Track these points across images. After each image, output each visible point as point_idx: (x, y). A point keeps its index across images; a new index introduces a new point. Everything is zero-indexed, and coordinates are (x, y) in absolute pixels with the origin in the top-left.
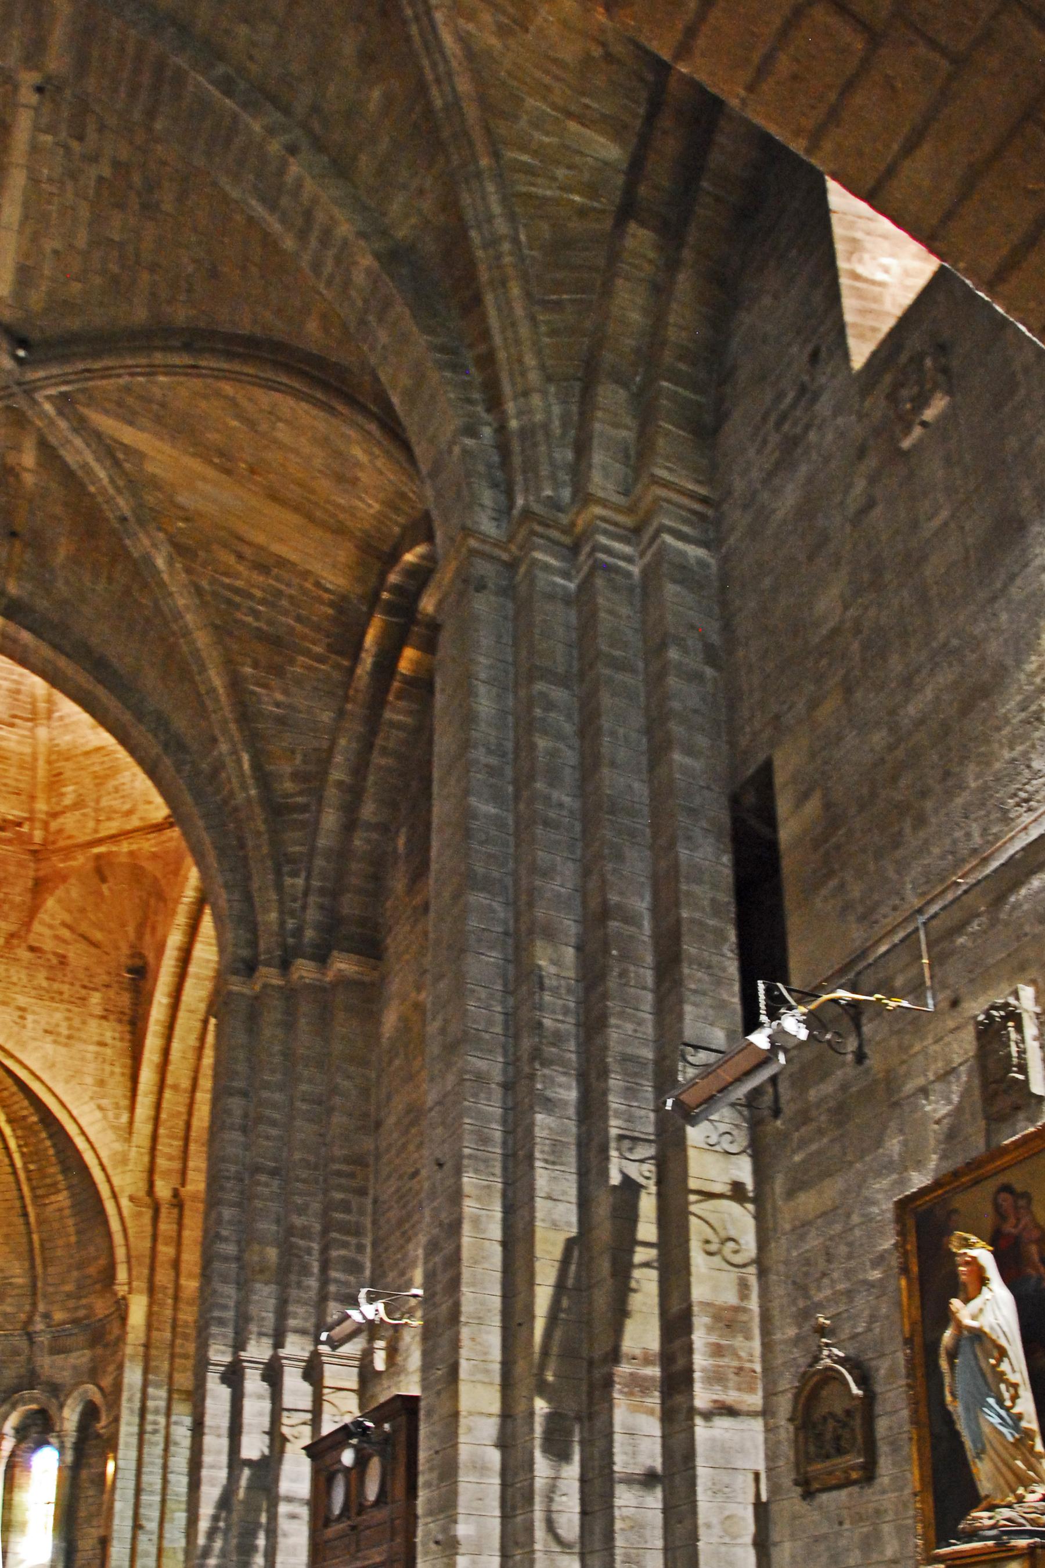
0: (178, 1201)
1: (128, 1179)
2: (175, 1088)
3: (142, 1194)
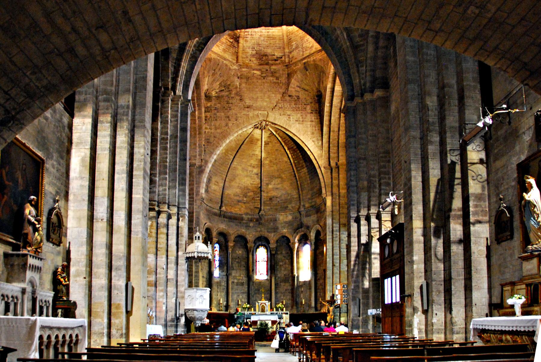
0: (338, 167)
1: (323, 162)
2: (333, 131)
3: (327, 165)
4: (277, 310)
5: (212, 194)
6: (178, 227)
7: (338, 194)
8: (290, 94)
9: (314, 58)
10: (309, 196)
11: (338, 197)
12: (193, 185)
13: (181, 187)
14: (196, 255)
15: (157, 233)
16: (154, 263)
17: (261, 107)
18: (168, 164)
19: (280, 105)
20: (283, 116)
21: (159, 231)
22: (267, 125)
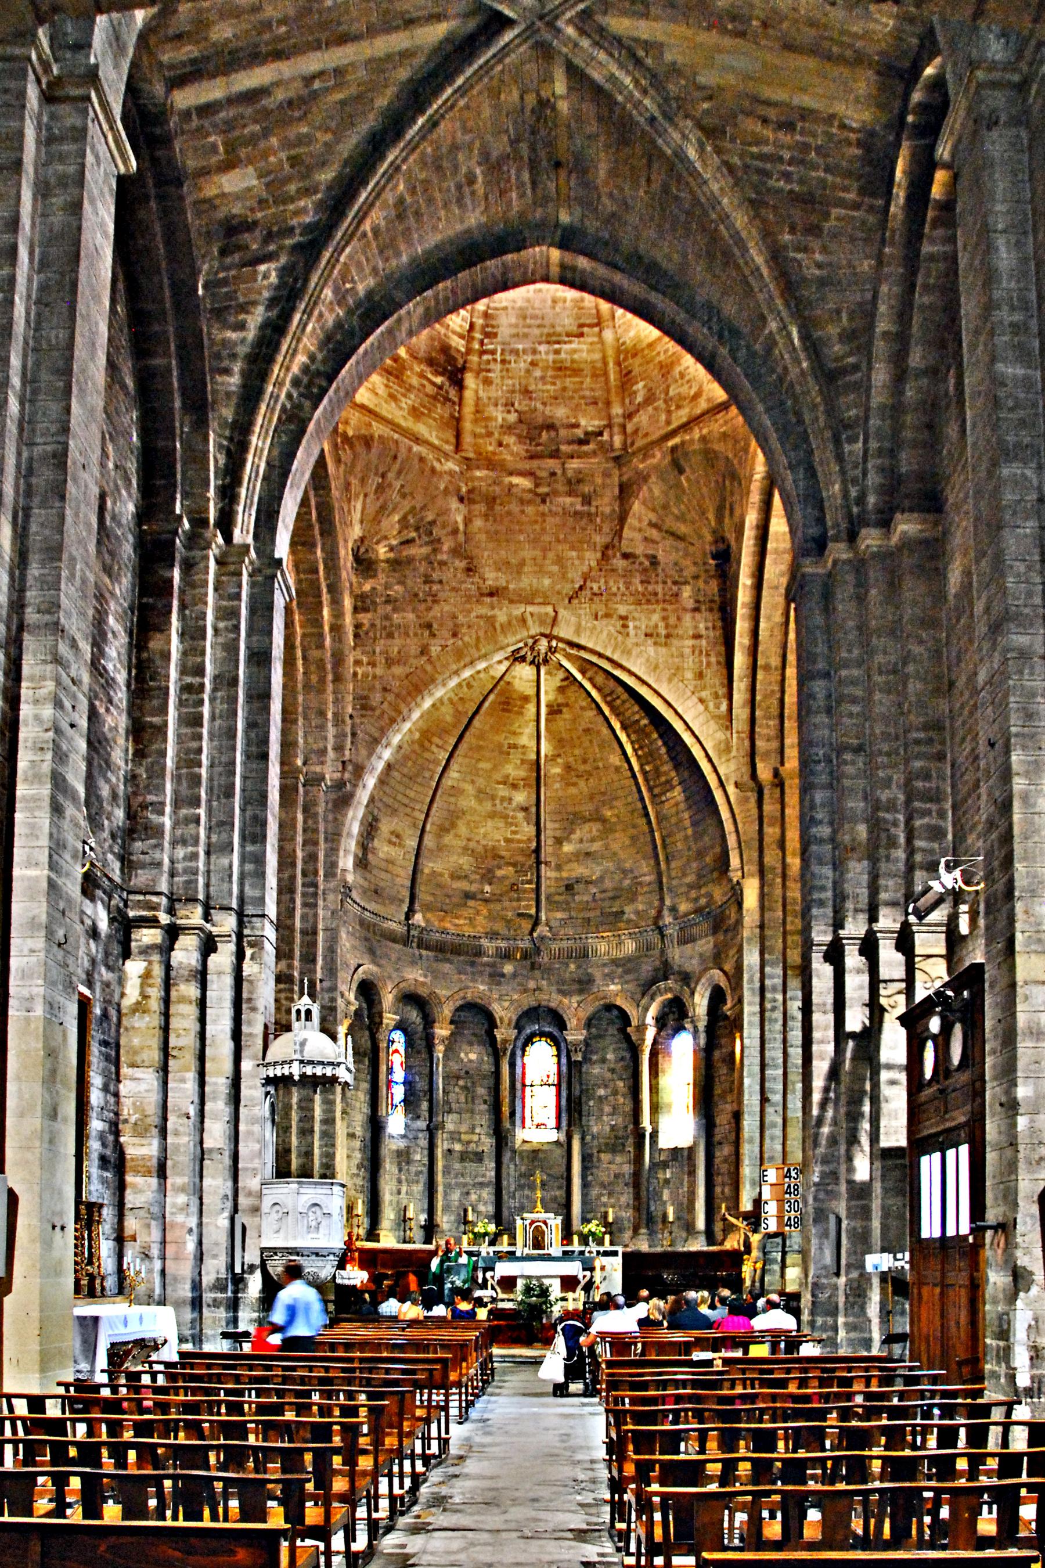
1: (733, 766)
2: (767, 668)
3: (746, 778)
4: (584, 1240)
5: (383, 875)
6: (239, 979)
7: (779, 871)
8: (629, 550)
9: (705, 431)
10: (690, 879)
11: (779, 880)
12: (316, 843)
13: (249, 848)
14: (296, 1070)
15: (167, 1001)
16: (153, 1099)
17: (535, 593)
18: (204, 772)
19: (595, 586)
20: (605, 622)
21: (173, 994)
22: (552, 650)
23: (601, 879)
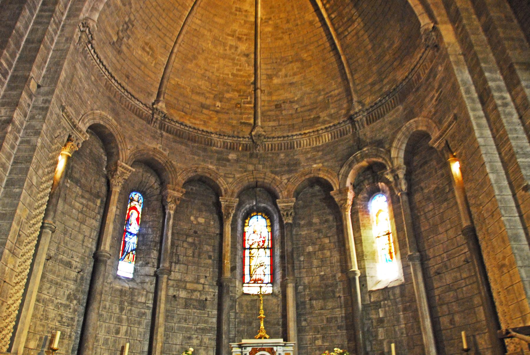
23: (301, 99)
